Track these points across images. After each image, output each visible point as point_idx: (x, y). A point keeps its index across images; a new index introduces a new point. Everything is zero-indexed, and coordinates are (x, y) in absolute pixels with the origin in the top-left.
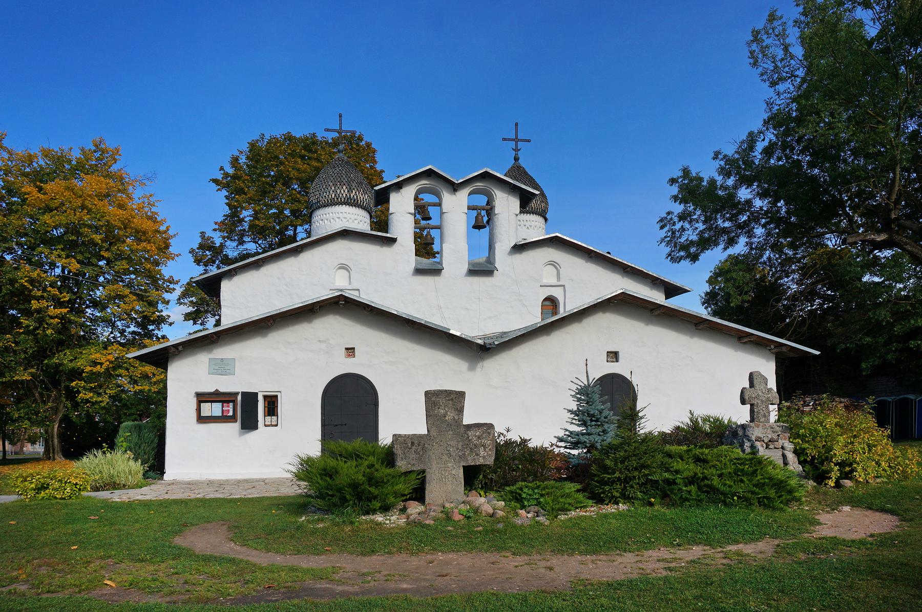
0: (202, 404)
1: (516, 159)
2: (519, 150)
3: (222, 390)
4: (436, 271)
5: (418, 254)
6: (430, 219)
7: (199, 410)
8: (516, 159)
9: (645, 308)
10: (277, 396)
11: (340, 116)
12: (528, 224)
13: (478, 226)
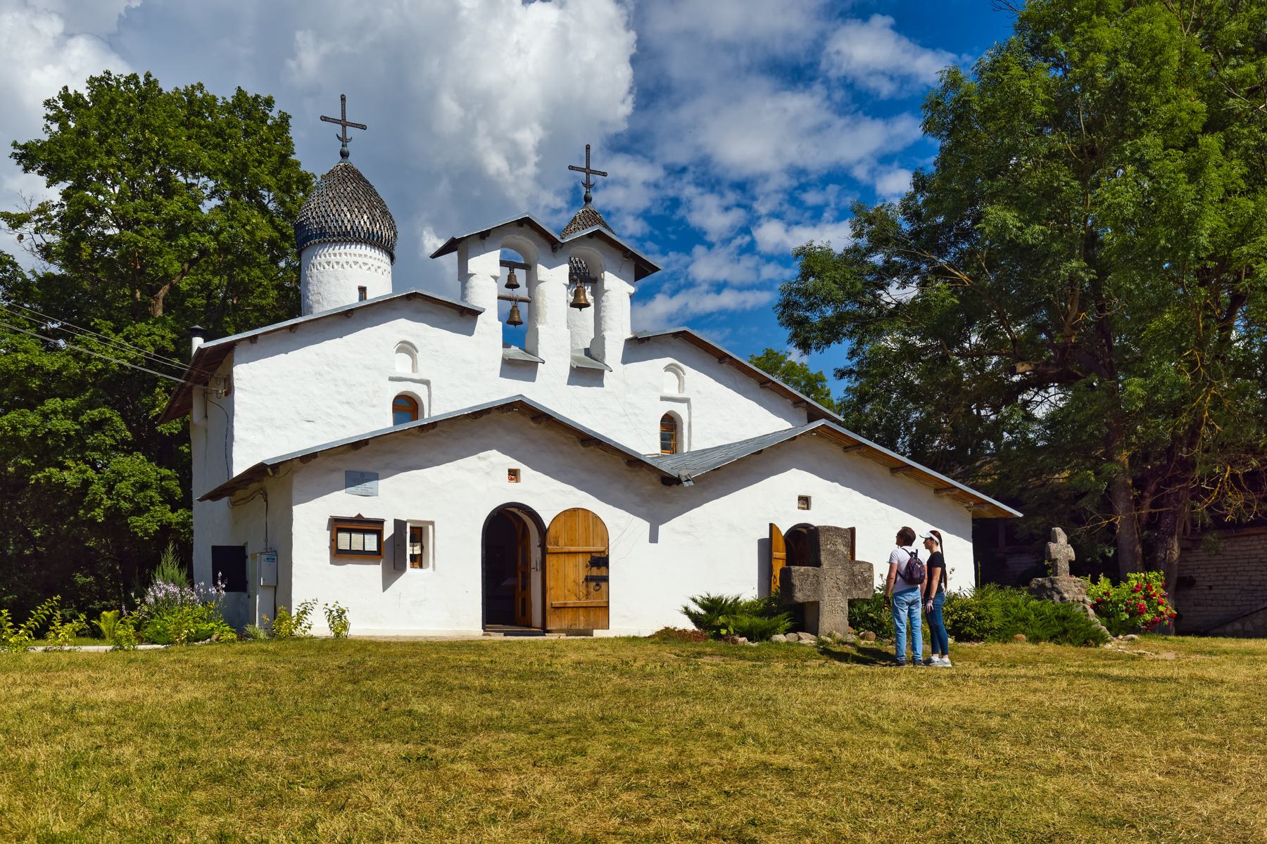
0: (340, 535)
3: (366, 515)
6: (517, 286)
7: (334, 541)
11: (343, 99)
13: (578, 304)
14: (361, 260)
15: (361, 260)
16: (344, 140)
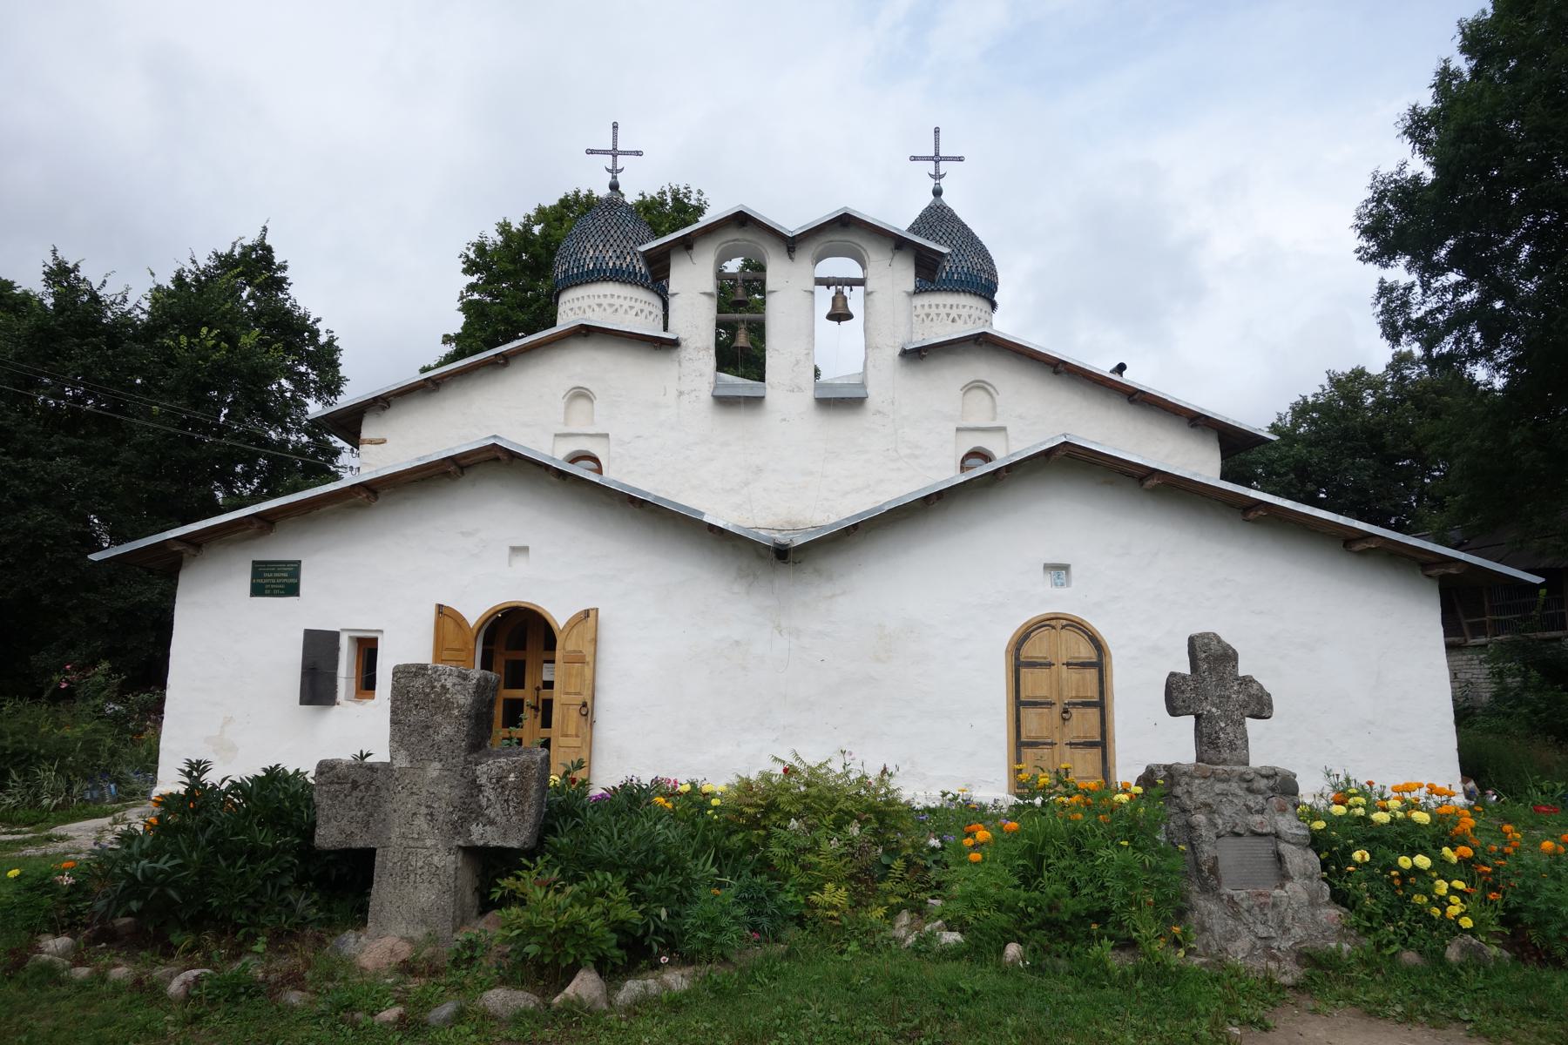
1: (937, 193)
2: (941, 177)
4: (756, 401)
5: (721, 367)
8: (937, 193)
9: (1131, 475)
10: (376, 640)
11: (615, 127)
12: (954, 313)
14: (605, 302)
15: (605, 302)
16: (614, 171)
